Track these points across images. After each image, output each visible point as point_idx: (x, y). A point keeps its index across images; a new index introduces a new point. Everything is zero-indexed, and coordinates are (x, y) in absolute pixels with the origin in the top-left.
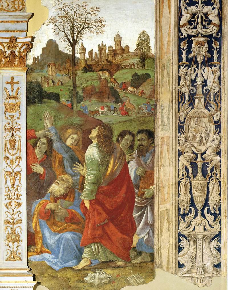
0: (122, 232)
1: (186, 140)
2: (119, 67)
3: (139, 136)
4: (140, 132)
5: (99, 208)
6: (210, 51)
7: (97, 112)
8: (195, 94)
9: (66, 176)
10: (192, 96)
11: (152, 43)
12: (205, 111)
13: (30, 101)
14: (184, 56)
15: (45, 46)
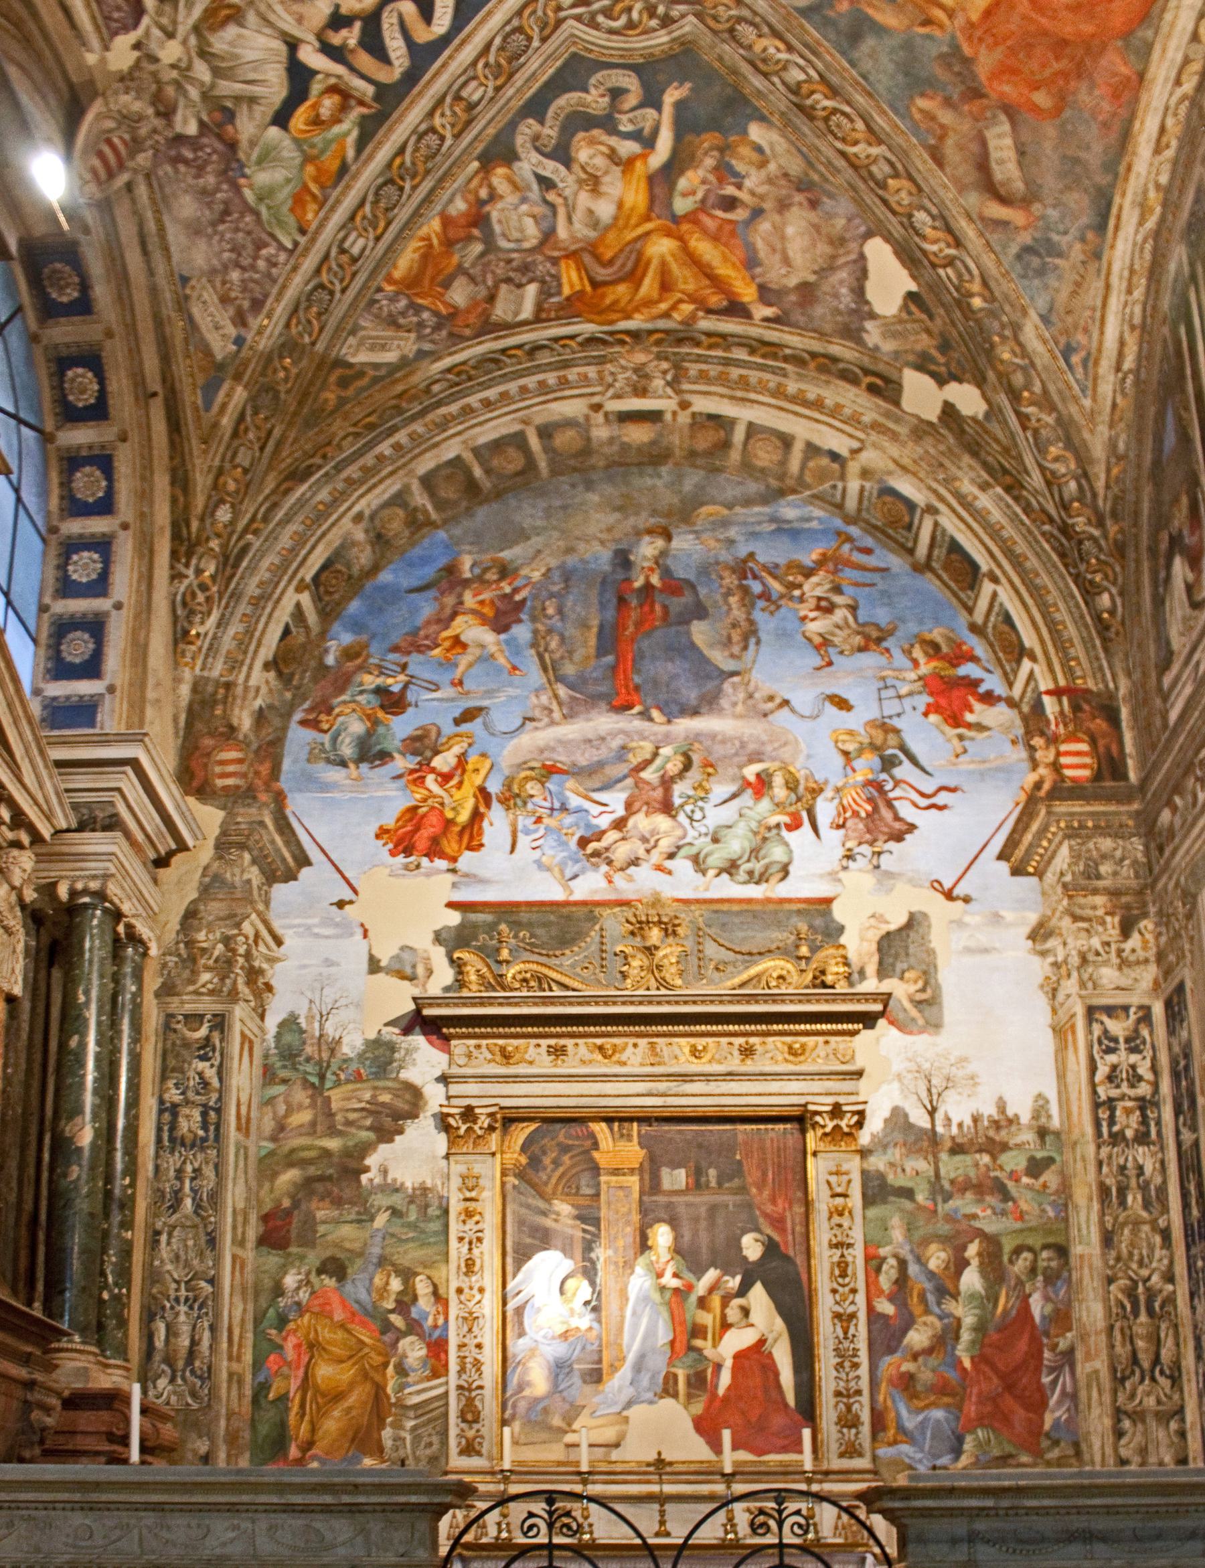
0: (1028, 1408)
1: (1118, 1259)
2: (1005, 1147)
3: (1045, 1254)
4: (1045, 1247)
5: (987, 1369)
6: (1144, 1121)
7: (974, 1217)
8: (1127, 1187)
9: (930, 1319)
10: (1122, 1191)
11: (1054, 1109)
12: (1145, 1214)
13: (869, 1200)
14: (1105, 1130)
15: (887, 1114)
